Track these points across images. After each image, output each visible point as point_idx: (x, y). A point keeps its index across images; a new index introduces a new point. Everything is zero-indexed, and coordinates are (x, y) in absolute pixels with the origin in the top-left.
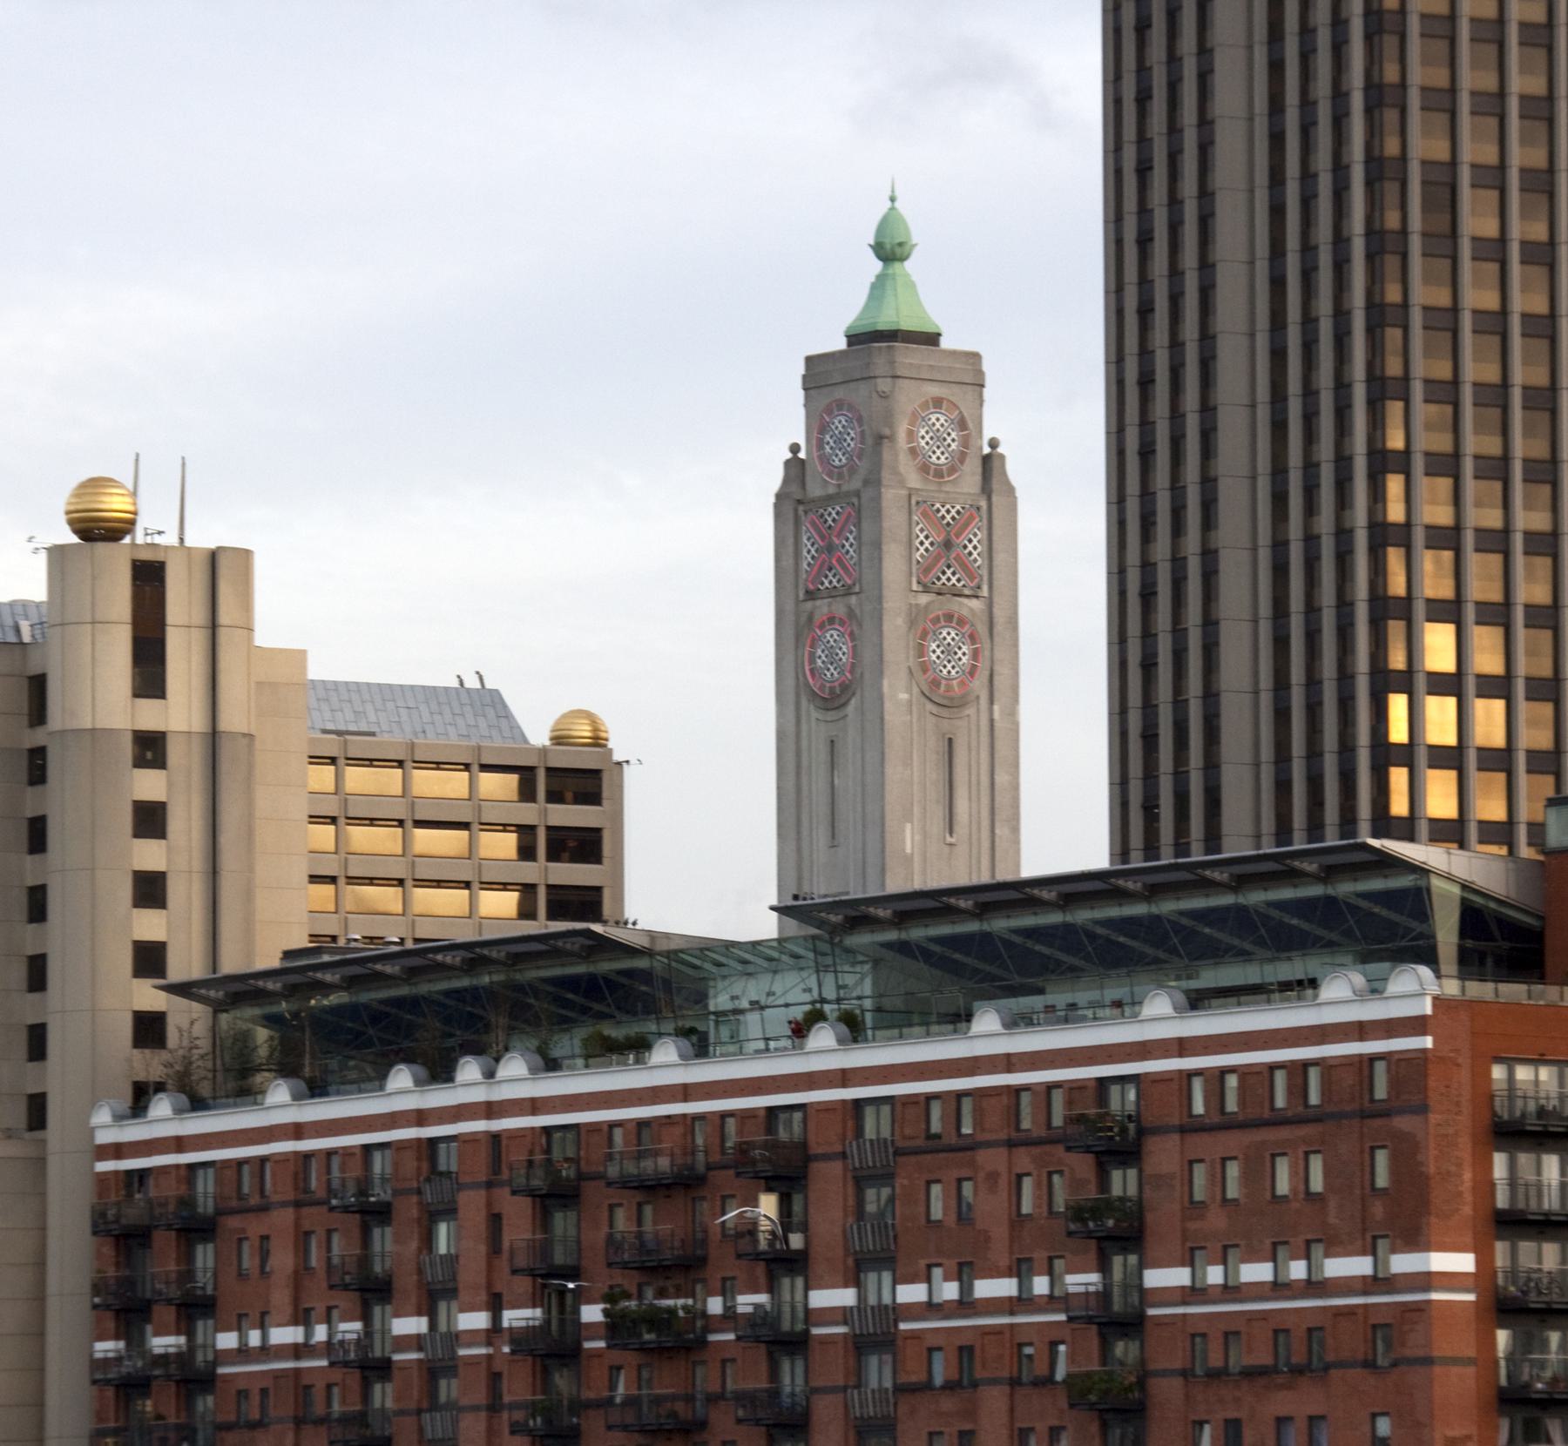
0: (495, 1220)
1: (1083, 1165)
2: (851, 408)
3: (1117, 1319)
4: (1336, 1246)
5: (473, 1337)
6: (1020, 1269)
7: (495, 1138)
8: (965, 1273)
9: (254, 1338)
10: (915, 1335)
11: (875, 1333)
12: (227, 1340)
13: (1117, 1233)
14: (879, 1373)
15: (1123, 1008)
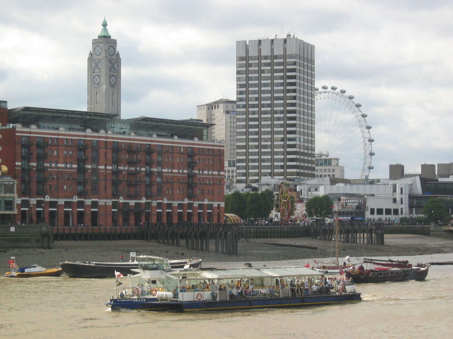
0: (106, 153)
1: (185, 156)
2: (113, 47)
3: (191, 176)
4: (213, 171)
5: (102, 169)
6: (179, 169)
7: (106, 142)
8: (173, 168)
9: (181, 171)
10: (165, 176)
11: (160, 174)
12: (48, 165)
13: (191, 166)
14: (159, 180)
15: (151, 136)
